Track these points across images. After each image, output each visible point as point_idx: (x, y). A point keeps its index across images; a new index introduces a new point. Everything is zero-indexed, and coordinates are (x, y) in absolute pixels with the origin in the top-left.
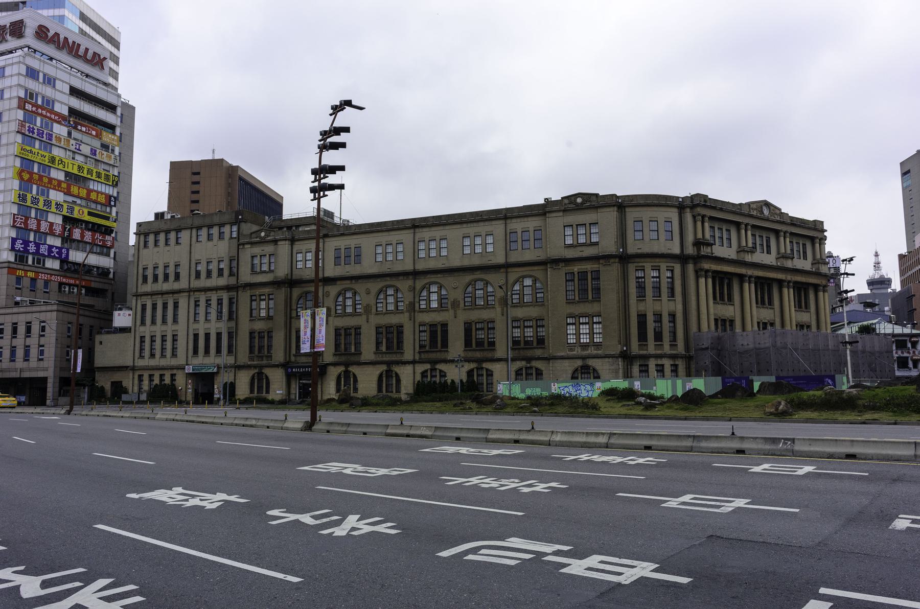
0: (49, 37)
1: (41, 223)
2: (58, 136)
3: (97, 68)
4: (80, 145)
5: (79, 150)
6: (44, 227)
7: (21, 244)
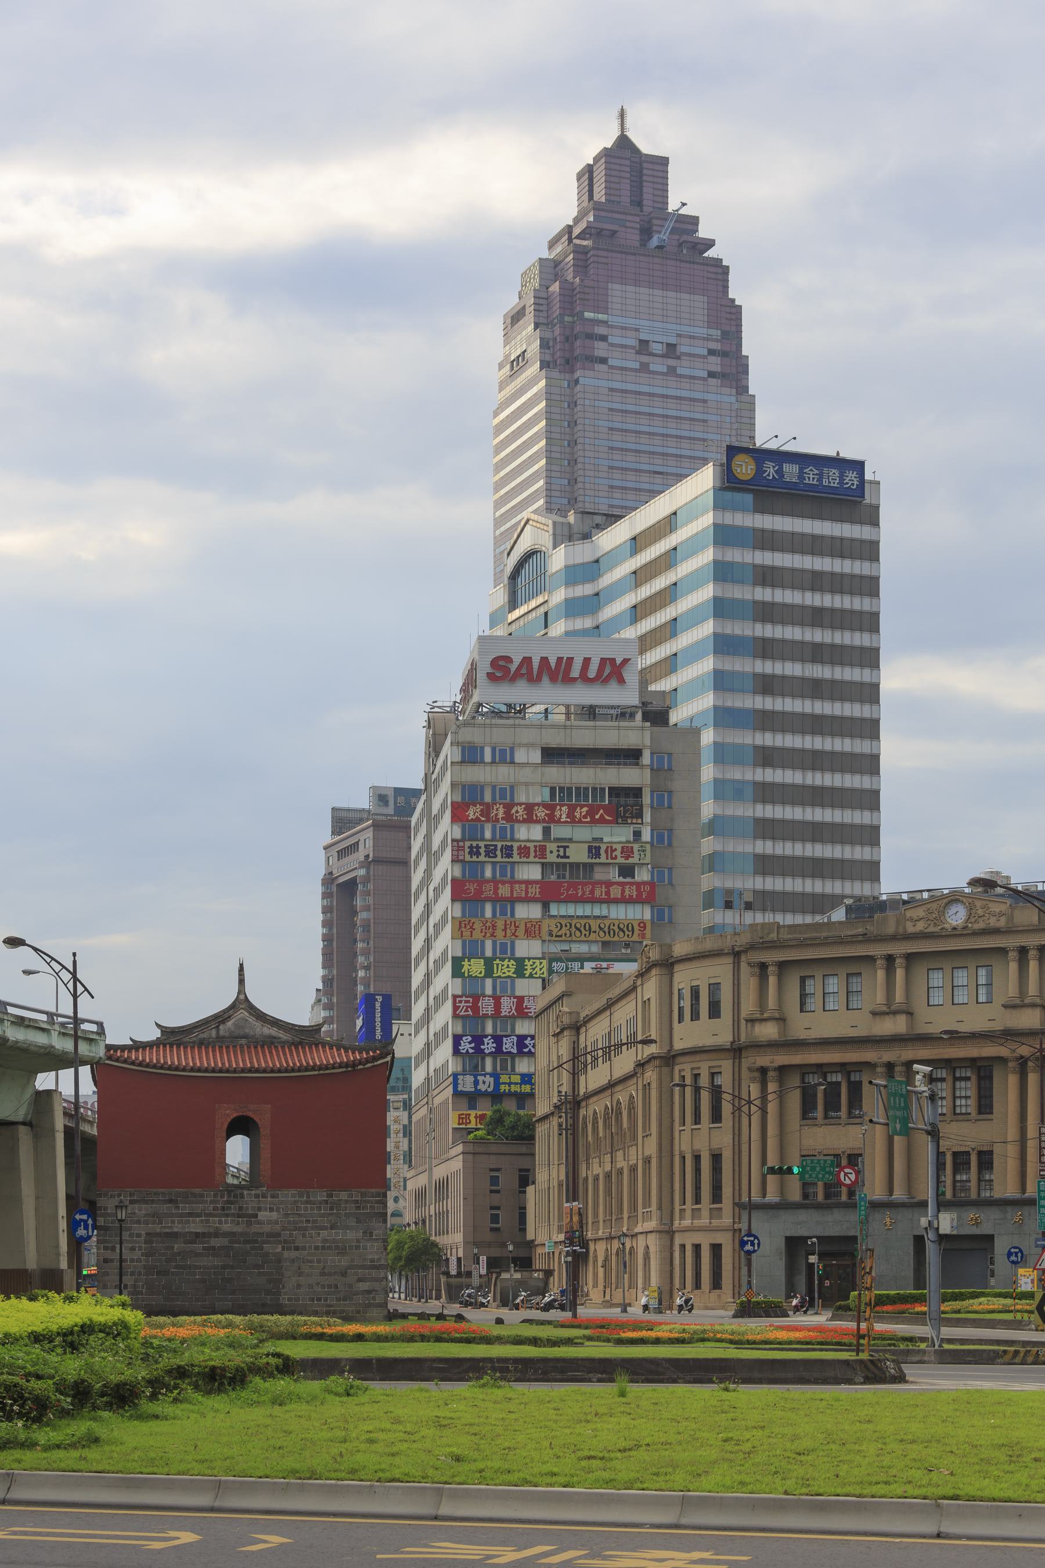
0: (512, 672)
1: (502, 1001)
2: (523, 844)
3: (613, 684)
4: (565, 847)
5: (565, 857)
6: (507, 1006)
7: (470, 1043)
